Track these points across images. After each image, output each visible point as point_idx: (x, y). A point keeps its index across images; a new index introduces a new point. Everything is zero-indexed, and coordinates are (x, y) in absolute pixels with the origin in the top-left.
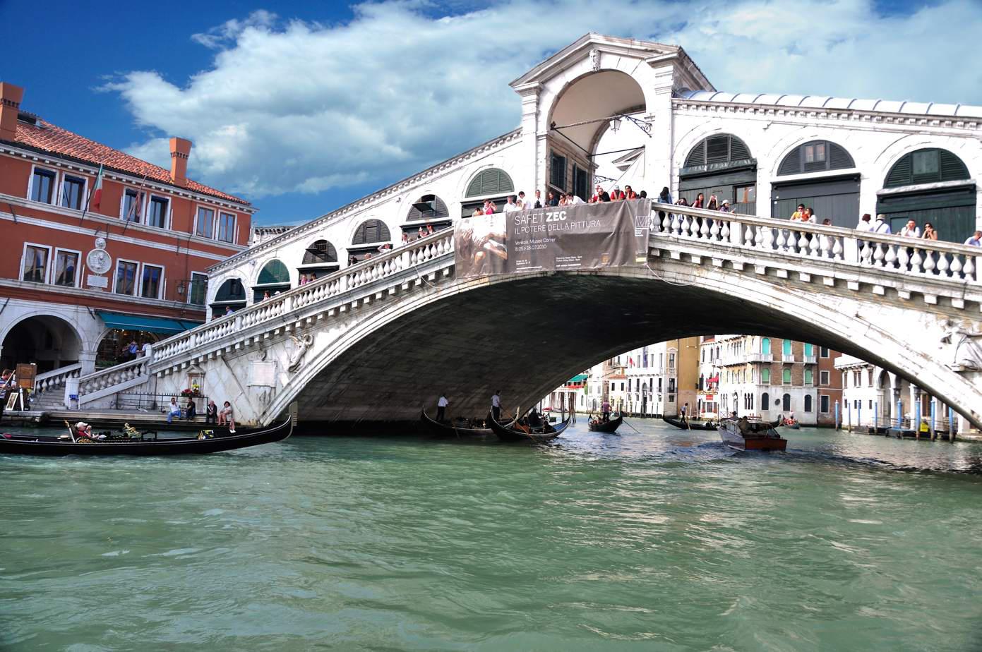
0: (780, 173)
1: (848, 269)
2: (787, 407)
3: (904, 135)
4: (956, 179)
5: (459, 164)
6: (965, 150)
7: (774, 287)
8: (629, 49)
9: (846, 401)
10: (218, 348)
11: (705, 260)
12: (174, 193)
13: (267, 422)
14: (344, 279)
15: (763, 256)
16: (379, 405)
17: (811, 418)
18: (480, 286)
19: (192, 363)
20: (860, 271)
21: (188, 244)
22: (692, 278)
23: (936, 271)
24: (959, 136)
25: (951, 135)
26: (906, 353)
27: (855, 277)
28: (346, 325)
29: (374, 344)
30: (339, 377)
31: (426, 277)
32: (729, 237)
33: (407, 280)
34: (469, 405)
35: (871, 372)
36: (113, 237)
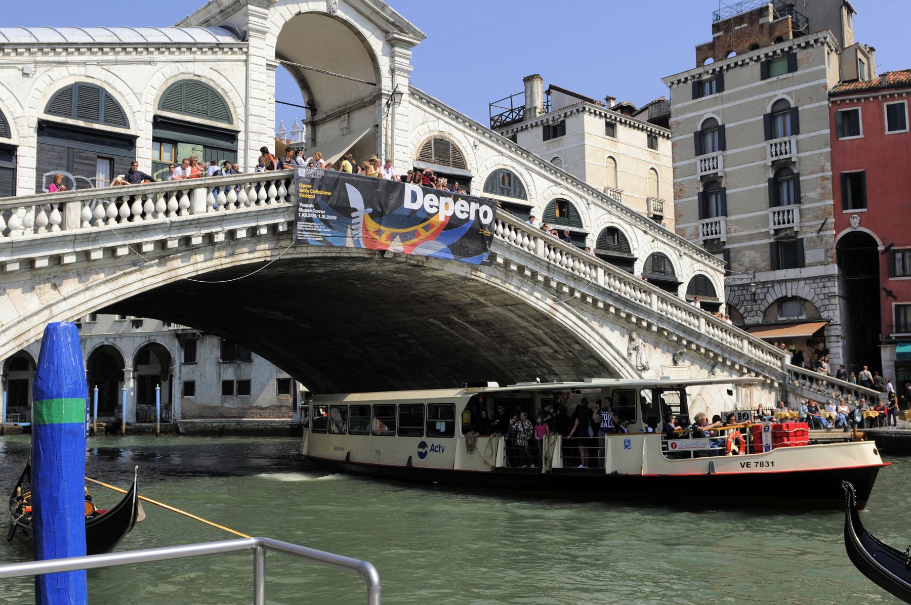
5: (145, 56)
6: (579, 205)
8: (374, 10)
18: (294, 256)
28: (55, 287)
33: (204, 232)
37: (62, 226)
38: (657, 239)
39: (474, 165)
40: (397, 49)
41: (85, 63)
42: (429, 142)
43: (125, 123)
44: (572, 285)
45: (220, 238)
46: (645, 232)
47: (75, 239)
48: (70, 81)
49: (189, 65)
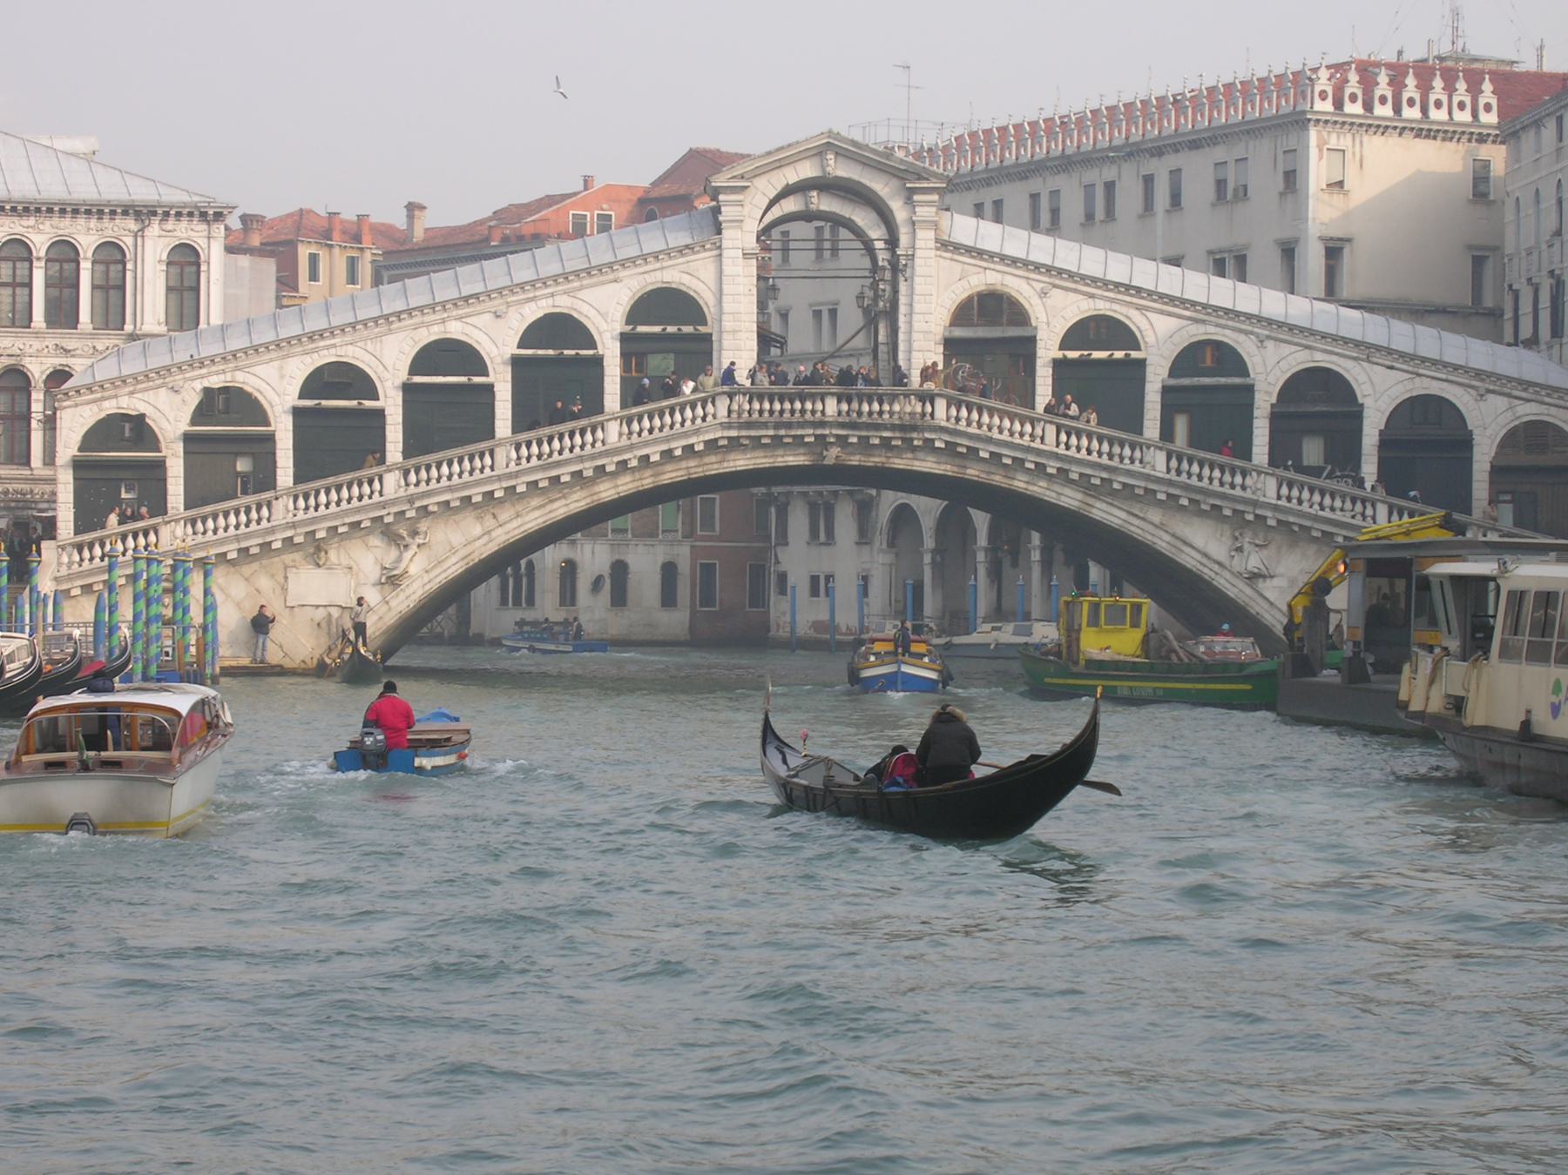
0: (1064, 345)
2: (619, 598)
5: (611, 276)
6: (1246, 346)
9: (783, 577)
10: (235, 546)
11: (1018, 462)
15: (1080, 462)
17: (676, 621)
20: (1170, 483)
22: (997, 478)
23: (1233, 486)
24: (1241, 331)
25: (1234, 329)
26: (1204, 560)
27: (1164, 489)
28: (494, 516)
32: (1042, 438)
33: (616, 459)
35: (864, 510)
37: (492, 468)
38: (1419, 375)
39: (1043, 318)
40: (916, 198)
41: (552, 295)
42: (970, 299)
43: (592, 344)
44: (1105, 475)
45: (634, 463)
46: (1391, 368)
47: (500, 478)
48: (540, 314)
49: (658, 274)
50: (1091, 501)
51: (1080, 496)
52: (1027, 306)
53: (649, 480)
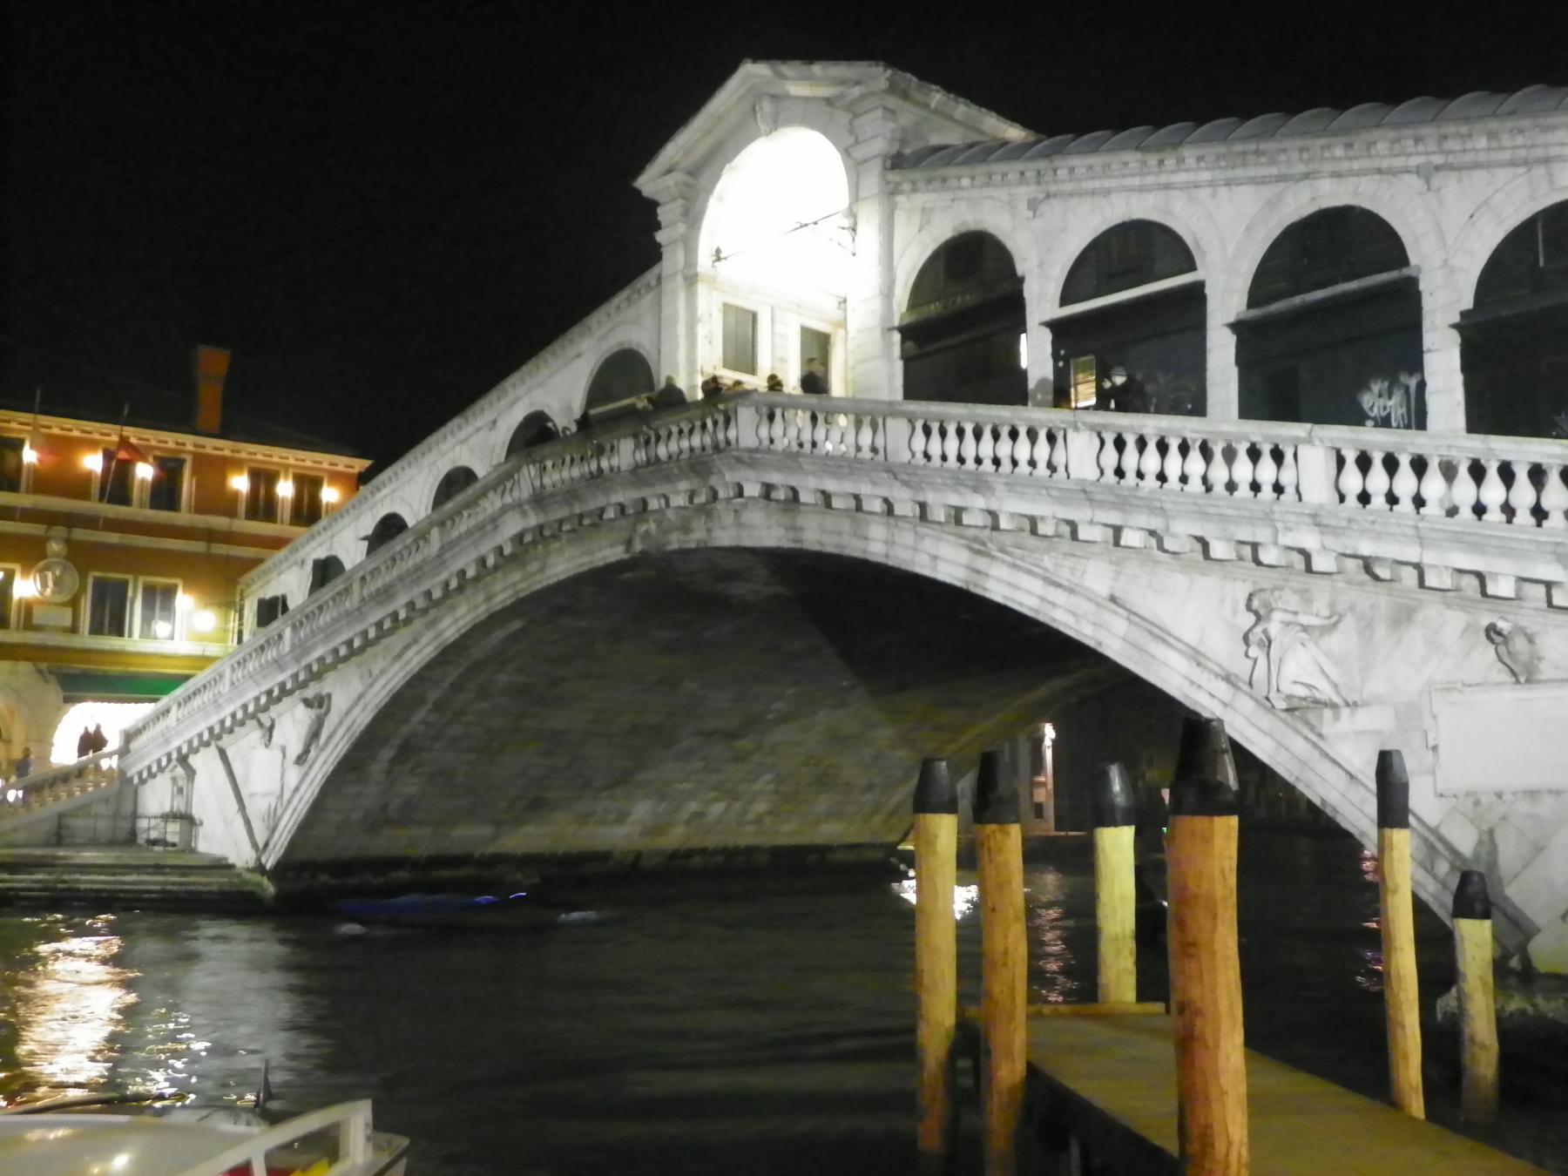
0: (1065, 300)
1: (1064, 497)
3: (1281, 185)
4: (1380, 272)
7: (971, 549)
12: (196, 445)
13: (270, 862)
14: (356, 587)
16: (518, 822)
18: (545, 583)
19: (174, 756)
21: (228, 537)
22: (845, 540)
29: (430, 706)
30: (389, 772)
31: (462, 573)
34: (750, 817)
36: (80, 534)
50: (981, 563)
51: (964, 556)
52: (1009, 244)
53: (482, 609)
